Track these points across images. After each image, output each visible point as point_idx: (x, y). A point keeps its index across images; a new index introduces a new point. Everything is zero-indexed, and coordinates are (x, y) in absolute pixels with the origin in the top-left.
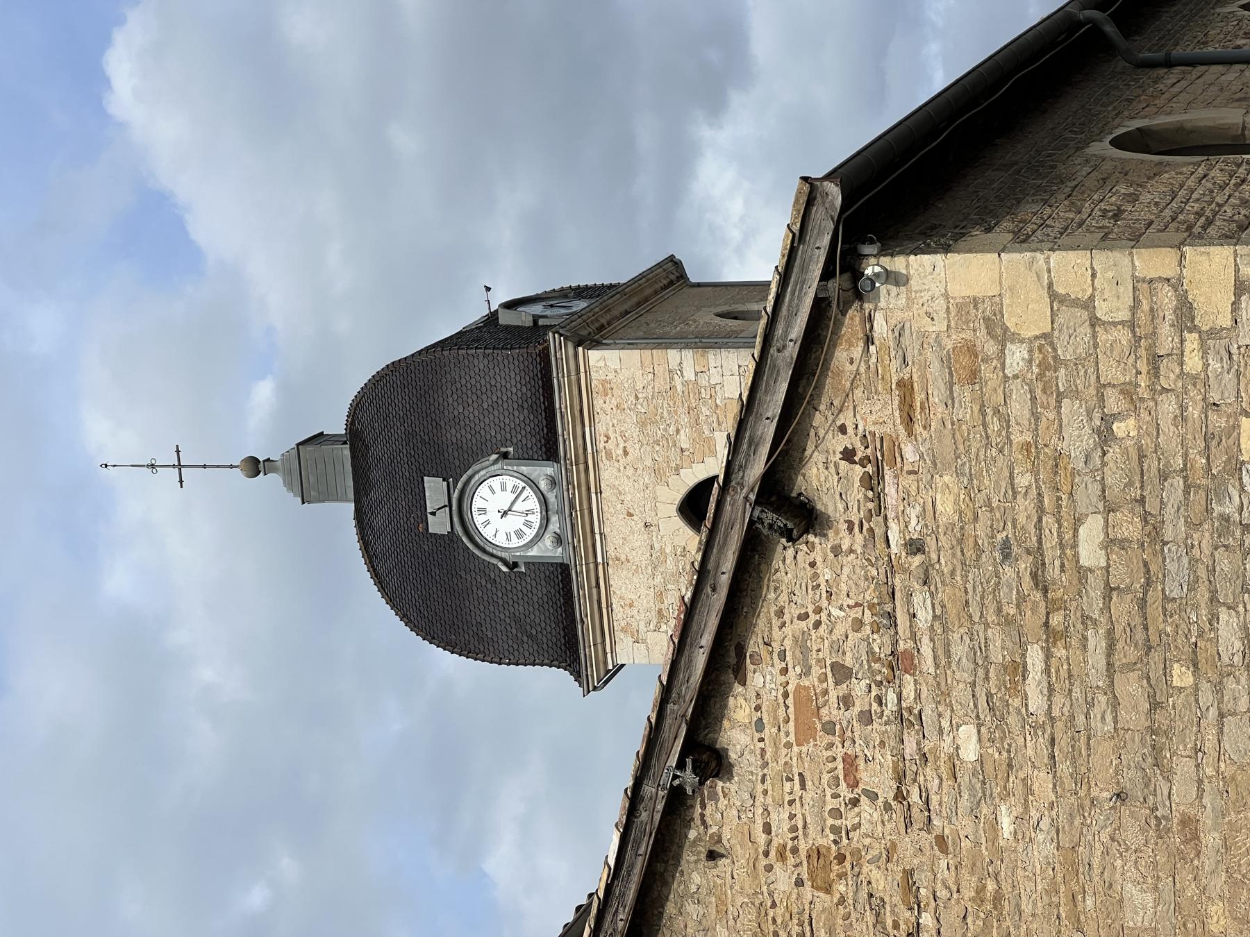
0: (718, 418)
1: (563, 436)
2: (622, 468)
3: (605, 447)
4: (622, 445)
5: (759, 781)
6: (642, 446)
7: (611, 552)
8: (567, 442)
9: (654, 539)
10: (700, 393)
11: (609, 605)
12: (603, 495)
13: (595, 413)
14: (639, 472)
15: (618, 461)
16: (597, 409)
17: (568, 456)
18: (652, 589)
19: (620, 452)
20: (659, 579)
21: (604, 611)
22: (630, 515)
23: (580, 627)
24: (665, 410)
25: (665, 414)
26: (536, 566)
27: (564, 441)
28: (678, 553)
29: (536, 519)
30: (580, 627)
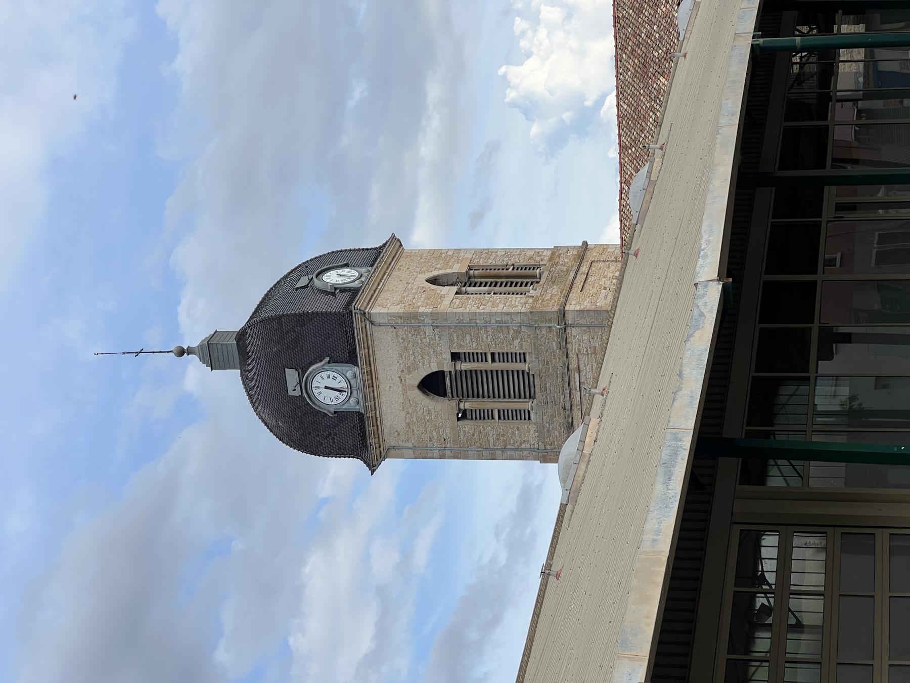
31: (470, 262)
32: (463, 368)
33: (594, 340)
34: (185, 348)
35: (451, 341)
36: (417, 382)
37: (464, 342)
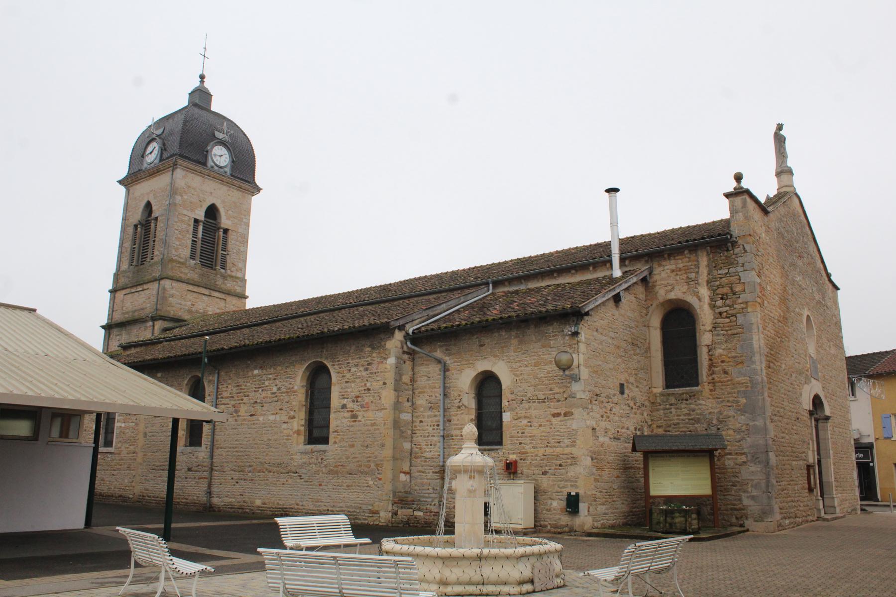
5: (705, 316)
7: (206, 180)
11: (193, 173)
20: (198, 190)
26: (206, 157)
29: (218, 163)
31: (232, 231)
32: (152, 224)
35: (162, 215)
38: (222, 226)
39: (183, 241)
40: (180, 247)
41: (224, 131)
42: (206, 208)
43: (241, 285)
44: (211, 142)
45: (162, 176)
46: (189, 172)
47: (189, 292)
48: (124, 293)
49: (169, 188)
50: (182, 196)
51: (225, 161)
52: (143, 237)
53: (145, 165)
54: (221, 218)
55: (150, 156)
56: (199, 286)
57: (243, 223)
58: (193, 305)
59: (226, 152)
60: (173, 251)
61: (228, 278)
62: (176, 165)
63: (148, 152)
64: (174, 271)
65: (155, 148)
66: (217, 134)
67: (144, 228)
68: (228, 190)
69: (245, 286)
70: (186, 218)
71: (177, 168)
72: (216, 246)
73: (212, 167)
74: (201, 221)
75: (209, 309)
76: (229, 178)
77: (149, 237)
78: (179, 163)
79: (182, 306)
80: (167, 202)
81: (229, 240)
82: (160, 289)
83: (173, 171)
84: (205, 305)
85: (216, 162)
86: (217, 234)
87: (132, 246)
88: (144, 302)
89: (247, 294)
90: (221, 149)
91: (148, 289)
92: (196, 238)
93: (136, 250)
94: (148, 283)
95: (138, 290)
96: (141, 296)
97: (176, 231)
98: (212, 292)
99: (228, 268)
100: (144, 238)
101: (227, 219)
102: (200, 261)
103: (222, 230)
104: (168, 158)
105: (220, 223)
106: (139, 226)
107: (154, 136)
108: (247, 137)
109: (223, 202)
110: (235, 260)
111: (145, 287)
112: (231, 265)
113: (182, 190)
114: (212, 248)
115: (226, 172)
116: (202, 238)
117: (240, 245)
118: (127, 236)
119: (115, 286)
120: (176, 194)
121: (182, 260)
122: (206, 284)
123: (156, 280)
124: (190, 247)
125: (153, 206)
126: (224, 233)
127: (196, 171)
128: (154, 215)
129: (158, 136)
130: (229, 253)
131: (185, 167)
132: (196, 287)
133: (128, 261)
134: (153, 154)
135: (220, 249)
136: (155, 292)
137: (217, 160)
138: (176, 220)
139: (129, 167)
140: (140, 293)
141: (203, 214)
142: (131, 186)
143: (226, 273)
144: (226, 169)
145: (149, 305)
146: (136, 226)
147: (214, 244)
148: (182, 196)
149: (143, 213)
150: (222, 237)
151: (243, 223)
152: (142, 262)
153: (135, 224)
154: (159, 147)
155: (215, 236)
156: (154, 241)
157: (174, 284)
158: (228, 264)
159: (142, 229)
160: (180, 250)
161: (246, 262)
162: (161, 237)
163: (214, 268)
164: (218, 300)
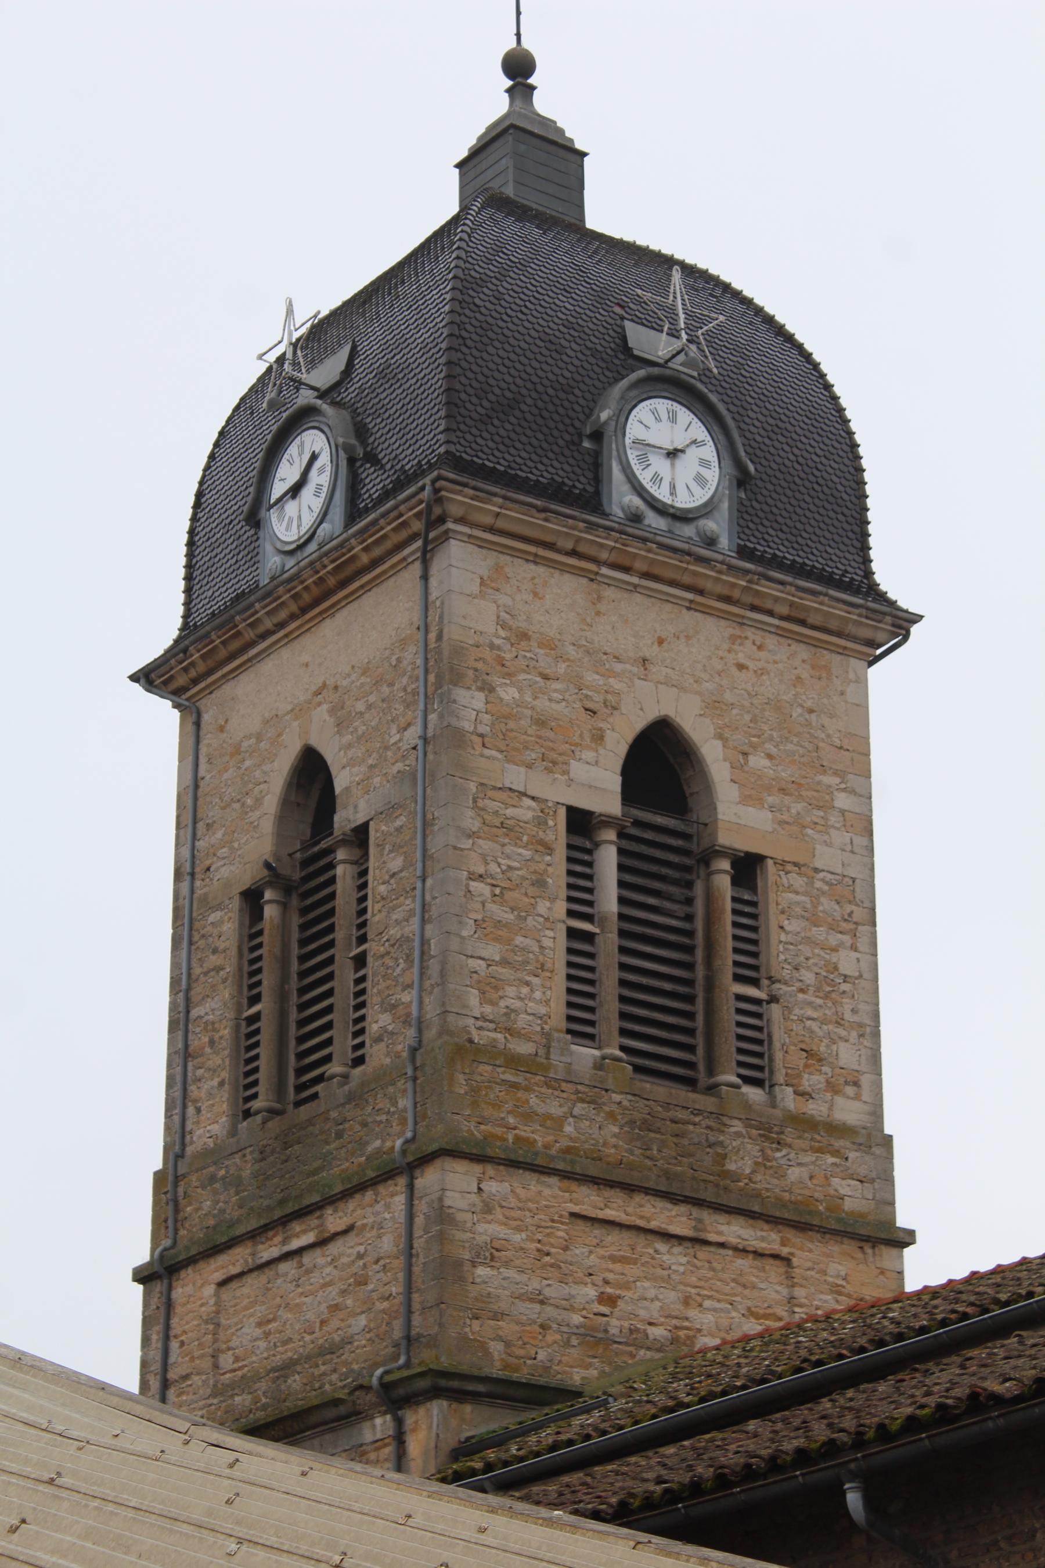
0: (787, 823)
1: (791, 584)
2: (721, 653)
3: (746, 638)
4: (751, 665)
6: (749, 694)
7: (609, 593)
8: (780, 587)
9: (628, 667)
10: (819, 808)
11: (536, 560)
12: (684, 611)
13: (790, 641)
14: (717, 679)
15: (729, 651)
16: (795, 646)
17: (763, 582)
18: (559, 637)
19: (741, 658)
20: (571, 651)
21: (532, 549)
22: (661, 642)
23: (539, 503)
24: (795, 748)
25: (790, 747)
27: (782, 583)
28: (609, 697)
29: (662, 494)
30: (539, 503)
32: (340, 870)
33: (381, 1274)
34: (531, 81)
35: (390, 810)
36: (314, 742)
37: (391, 851)
38: (725, 838)
39: (519, 940)
40: (504, 972)
41: (674, 322)
42: (623, 749)
43: (862, 1171)
44: (617, 381)
45: (368, 600)
46: (514, 553)
47: (581, 1225)
48: (219, 1276)
49: (413, 656)
50: (488, 689)
51: (700, 480)
52: (295, 951)
53: (272, 562)
54: (708, 788)
55: (291, 507)
56: (629, 1188)
57: (834, 819)
58: (611, 1301)
59: (699, 431)
60: (473, 998)
61: (789, 1135)
62: (442, 520)
63: (278, 489)
64: (488, 1111)
65: (314, 457)
66: (639, 338)
67: (295, 901)
68: (733, 639)
69: (887, 1178)
70: (526, 811)
71: (446, 536)
72: (699, 954)
73: (636, 518)
74: (607, 822)
75: (703, 1319)
76: (731, 567)
77: (331, 944)
78: (454, 510)
79: (550, 1311)
80: (413, 735)
81: (773, 918)
82: (419, 1220)
83: (426, 558)
84: (671, 1296)
85: (653, 490)
86: (699, 889)
87: (239, 1011)
88: (335, 1308)
89: (903, 1220)
90: (673, 418)
91: (345, 1232)
92: (589, 918)
93: (267, 1028)
94: (347, 1194)
95: (295, 1244)
96: (316, 1278)
97: (475, 886)
98: (706, 1215)
99: (780, 1077)
100: (303, 959)
101: (746, 800)
102: (623, 1048)
103: (725, 865)
104: (387, 494)
105: (709, 825)
106: (268, 895)
107: (306, 397)
108: (799, 347)
109: (714, 706)
110: (814, 1026)
111: (334, 1220)
112: (797, 1059)
113: (487, 654)
114: (681, 989)
115: (711, 542)
116: (622, 917)
117: (834, 939)
118: (214, 960)
119: (167, 1242)
120: (457, 679)
121: (524, 1048)
122: (667, 1175)
123: (387, 1175)
124: (562, 970)
125: (334, 771)
126: (735, 882)
127: (550, 546)
128: (344, 819)
129: (323, 395)
130: (780, 989)
131: (491, 529)
132: (617, 1197)
133: (225, 1094)
134: (307, 493)
135: (729, 970)
136: (388, 1244)
137: (657, 479)
138: (470, 821)
139: (188, 591)
140: (307, 1259)
141: (615, 783)
142: (210, 690)
143: (773, 1105)
144: (710, 525)
145: (362, 1321)
146: (252, 898)
147: (690, 950)
148: (488, 689)
149: (282, 818)
150: (729, 905)
151: (834, 819)
152: (300, 1088)
153: (246, 883)
154: (336, 450)
155: (689, 901)
156: (360, 961)
157: (492, 1187)
158: (779, 1055)
159: (284, 906)
160: (511, 991)
161: (876, 1034)
162: (394, 932)
163: (703, 1080)
164: (743, 1263)
